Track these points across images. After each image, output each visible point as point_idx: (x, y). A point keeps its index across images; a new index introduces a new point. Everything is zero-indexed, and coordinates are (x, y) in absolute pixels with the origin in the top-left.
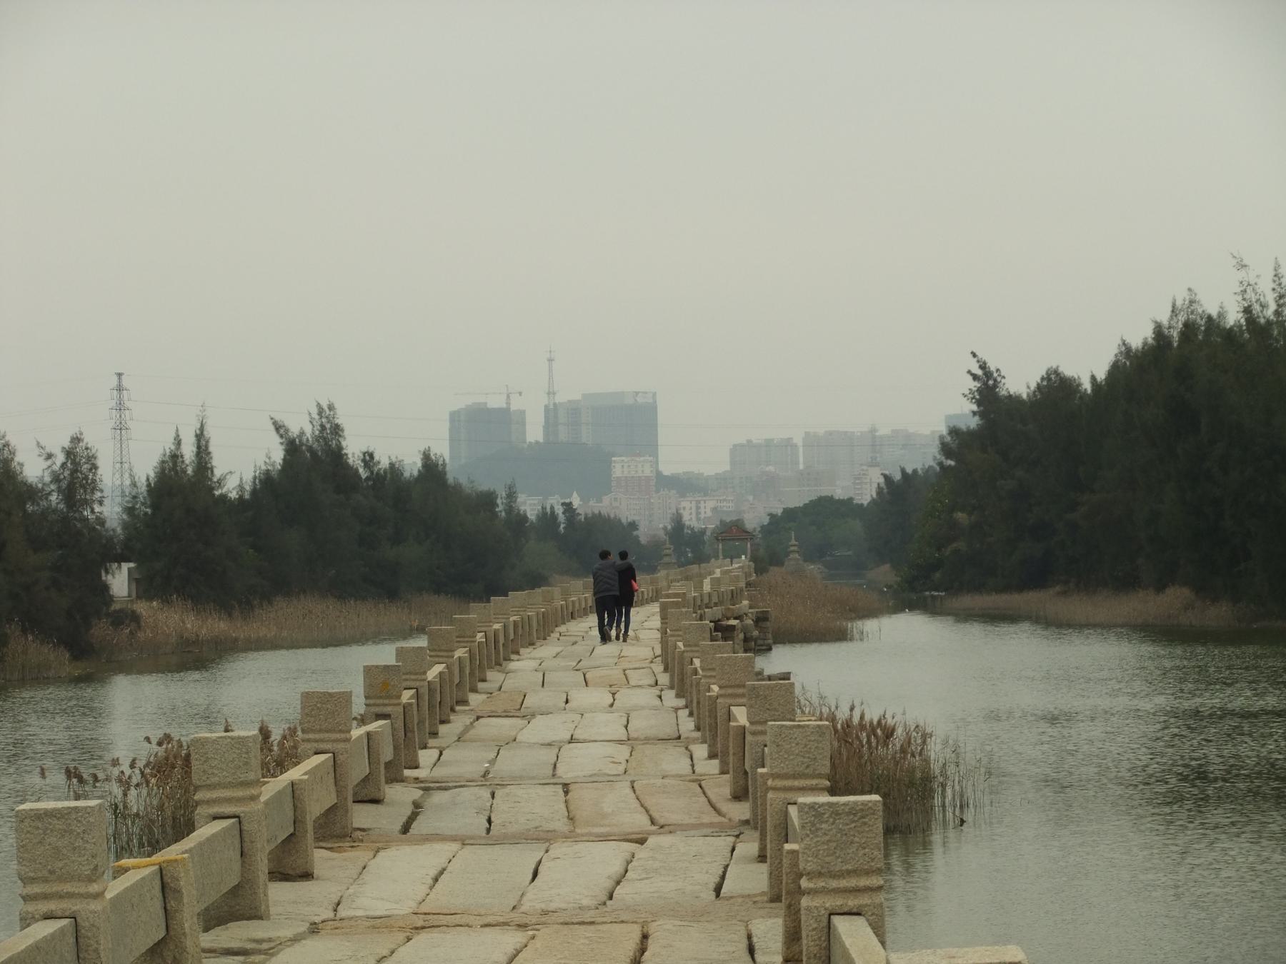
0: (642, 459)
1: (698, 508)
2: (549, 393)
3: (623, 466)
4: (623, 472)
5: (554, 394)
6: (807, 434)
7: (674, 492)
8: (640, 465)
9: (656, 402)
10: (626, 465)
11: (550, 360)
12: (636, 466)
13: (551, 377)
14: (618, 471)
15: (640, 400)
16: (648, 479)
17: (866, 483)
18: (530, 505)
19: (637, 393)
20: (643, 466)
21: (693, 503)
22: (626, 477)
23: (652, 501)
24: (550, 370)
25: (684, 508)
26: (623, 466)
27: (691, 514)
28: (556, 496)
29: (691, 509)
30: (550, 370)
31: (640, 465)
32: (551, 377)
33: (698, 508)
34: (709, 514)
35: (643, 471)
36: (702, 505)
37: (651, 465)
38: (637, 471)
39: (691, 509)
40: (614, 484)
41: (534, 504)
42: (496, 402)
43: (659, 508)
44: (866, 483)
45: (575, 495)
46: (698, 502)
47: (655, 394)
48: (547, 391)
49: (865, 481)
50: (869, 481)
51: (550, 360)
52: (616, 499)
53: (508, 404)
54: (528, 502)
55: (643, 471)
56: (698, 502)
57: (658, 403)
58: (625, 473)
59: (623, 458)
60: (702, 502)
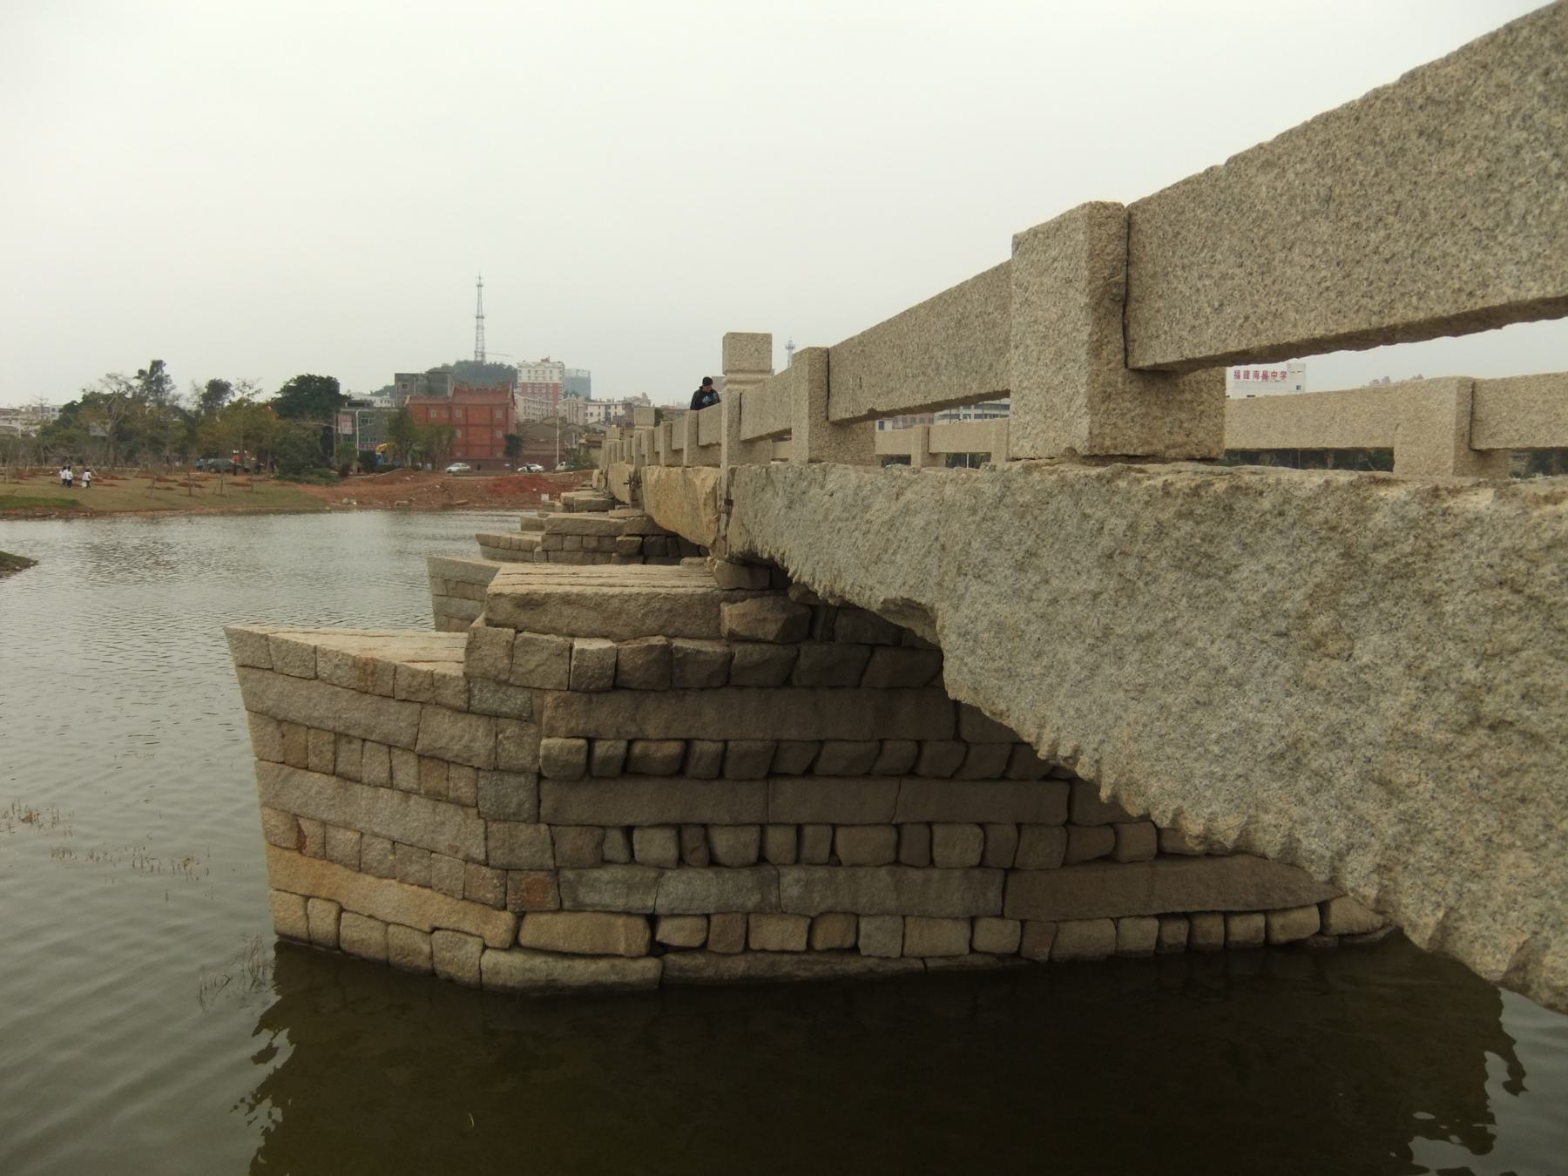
1: (607, 414)
2: (478, 317)
3: (529, 371)
5: (483, 317)
8: (548, 372)
10: (532, 372)
11: (480, 286)
13: (479, 303)
16: (556, 385)
20: (551, 372)
21: (603, 408)
22: (534, 384)
23: (557, 407)
24: (480, 295)
25: (591, 414)
26: (529, 371)
29: (599, 414)
30: (480, 295)
31: (548, 372)
32: (479, 303)
35: (551, 378)
39: (599, 414)
46: (608, 407)
47: (589, 373)
48: (476, 313)
51: (480, 286)
55: (551, 378)
58: (533, 378)
60: (613, 407)
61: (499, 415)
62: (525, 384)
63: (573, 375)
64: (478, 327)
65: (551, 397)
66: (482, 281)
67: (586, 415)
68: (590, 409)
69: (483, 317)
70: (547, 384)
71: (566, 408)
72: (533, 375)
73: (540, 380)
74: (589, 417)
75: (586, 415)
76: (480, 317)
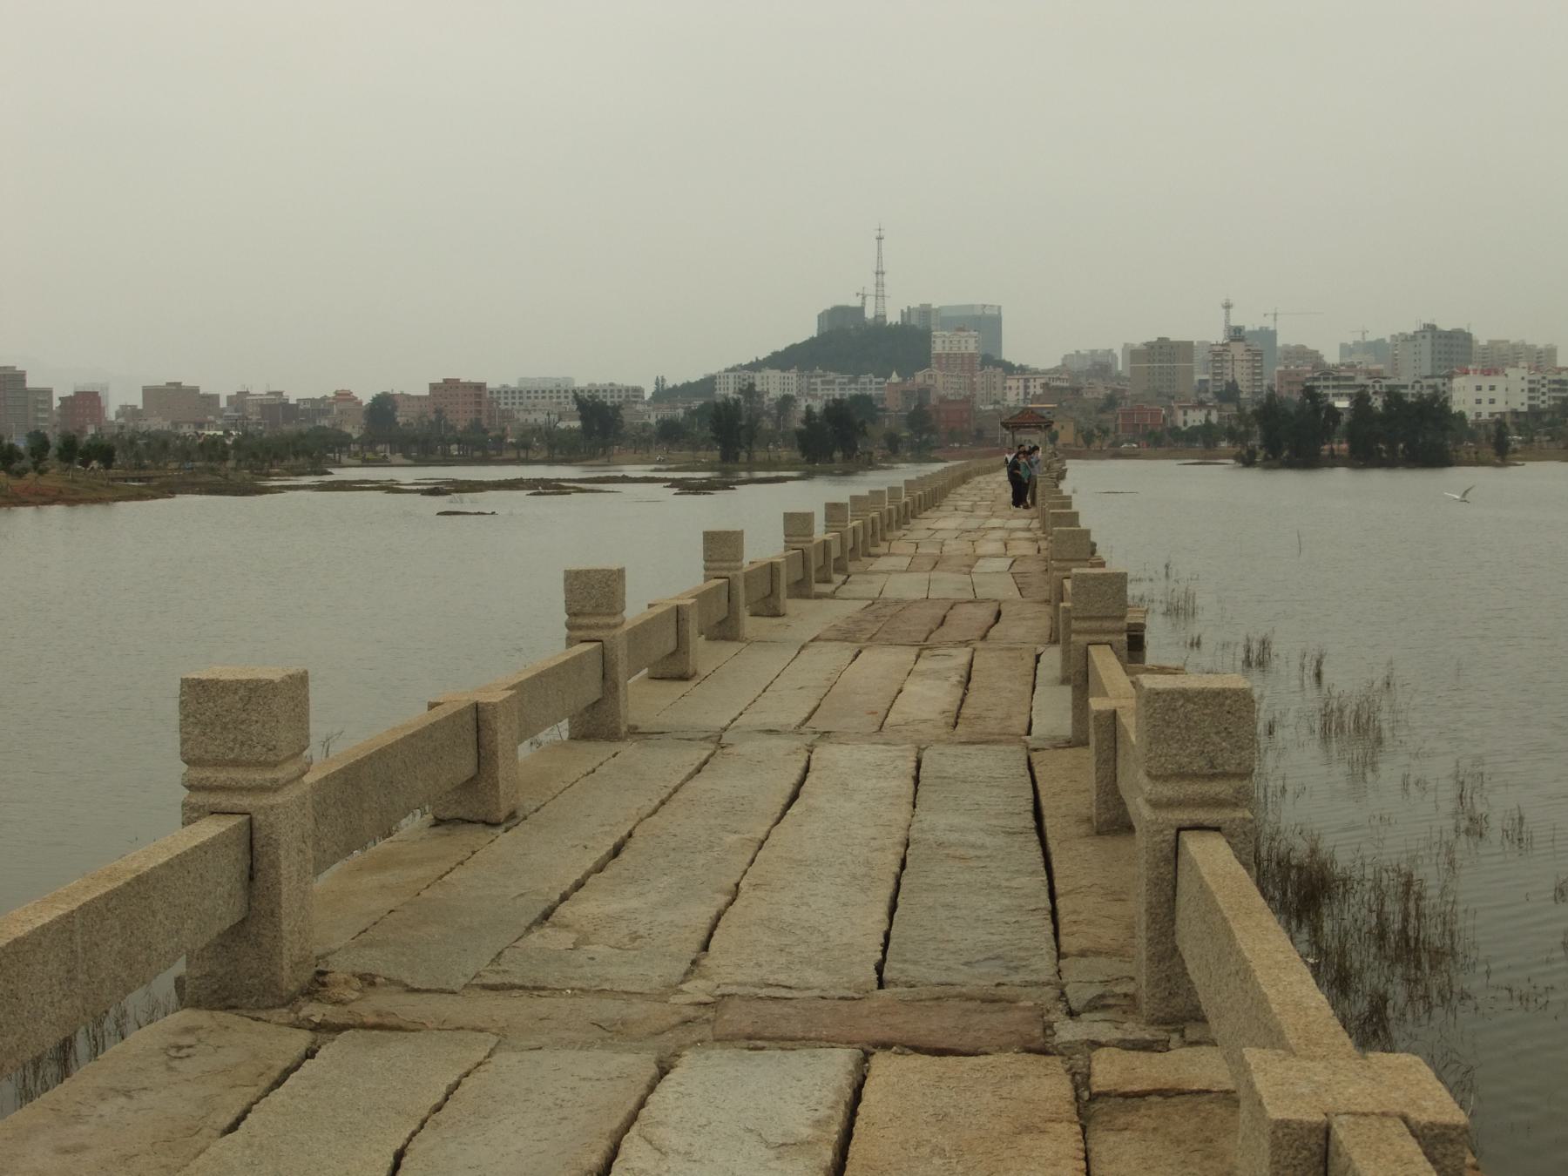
0: (966, 334)
1: (1026, 387)
2: (877, 273)
3: (944, 342)
4: (944, 348)
5: (883, 273)
6: (1126, 345)
7: (1000, 369)
9: (1000, 313)
10: (947, 342)
11: (880, 238)
12: (959, 341)
13: (879, 257)
14: (938, 347)
15: (988, 312)
17: (1227, 361)
18: (840, 384)
19: (985, 306)
21: (1022, 381)
22: (948, 354)
24: (879, 249)
25: (1010, 388)
26: (944, 342)
27: (1018, 394)
28: (870, 375)
29: (1018, 388)
30: (879, 249)
32: (879, 257)
33: (1026, 387)
34: (1039, 391)
36: (1031, 384)
37: (976, 341)
38: (959, 348)
39: (1018, 388)
40: (933, 361)
41: (844, 383)
42: (855, 302)
43: (983, 389)
44: (1227, 361)
45: (894, 375)
46: (1027, 380)
47: (1000, 308)
48: (875, 270)
49: (1226, 358)
50: (1230, 358)
51: (880, 238)
52: (930, 376)
53: (863, 303)
54: (837, 381)
56: (1027, 380)
57: (1002, 313)
59: (945, 333)
61: (965, 415)
62: (939, 355)
63: (979, 312)
64: (877, 285)
65: (966, 368)
66: (883, 233)
67: (1005, 388)
68: (1009, 383)
69: (883, 273)
70: (962, 354)
71: (984, 380)
72: (947, 345)
73: (955, 350)
74: (1007, 391)
75: (1005, 388)
76: (880, 273)
